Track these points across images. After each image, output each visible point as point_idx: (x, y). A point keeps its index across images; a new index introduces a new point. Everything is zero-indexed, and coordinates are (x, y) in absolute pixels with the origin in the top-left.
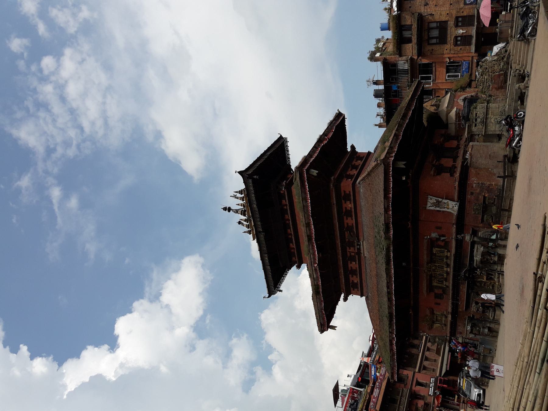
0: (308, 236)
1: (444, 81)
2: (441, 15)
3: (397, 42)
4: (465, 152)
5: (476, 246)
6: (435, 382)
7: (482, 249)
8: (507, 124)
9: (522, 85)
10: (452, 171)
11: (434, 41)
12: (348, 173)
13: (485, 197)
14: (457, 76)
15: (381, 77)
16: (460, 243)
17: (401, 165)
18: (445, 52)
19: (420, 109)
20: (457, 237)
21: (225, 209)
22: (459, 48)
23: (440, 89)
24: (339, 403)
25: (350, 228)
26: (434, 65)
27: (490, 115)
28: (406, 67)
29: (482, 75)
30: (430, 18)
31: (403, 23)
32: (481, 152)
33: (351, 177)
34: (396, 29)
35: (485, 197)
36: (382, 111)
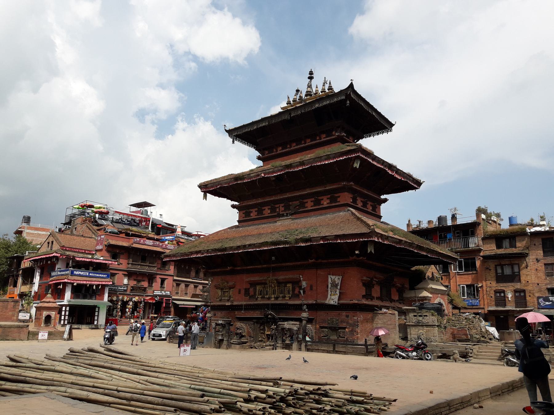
0: (291, 164)
1: (458, 283)
2: (527, 275)
3: (497, 235)
4: (388, 308)
5: (298, 323)
6: (166, 296)
7: (295, 328)
8: (418, 345)
9: (457, 356)
10: (367, 296)
11: (499, 271)
12: (358, 198)
13: (345, 328)
14: (464, 295)
15: (459, 221)
16: (299, 308)
17: (370, 249)
18: (488, 282)
19: (428, 262)
20: (304, 305)
21: (311, 73)
22: (493, 296)
23: (450, 280)
24: (134, 209)
25: (302, 205)
26: (475, 272)
27: (426, 328)
28: (472, 246)
29: (466, 318)
30: (524, 265)
31: (517, 239)
32: (389, 323)
33: (355, 201)
34: (511, 233)
35: (345, 328)
36: (425, 225)
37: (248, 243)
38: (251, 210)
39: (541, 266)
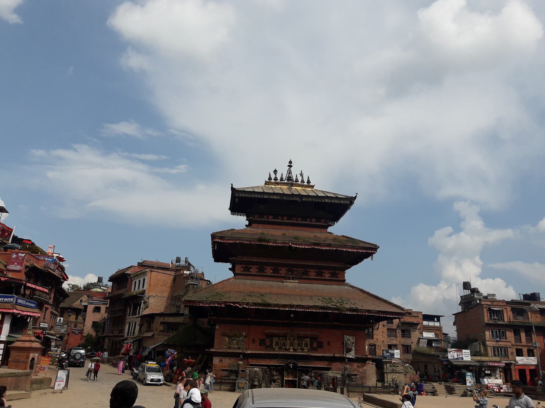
0: (320, 243)
7: (339, 376)
21: (290, 162)
25: (306, 273)
35: (356, 375)
37: (295, 303)
38: (251, 266)
39: (385, 329)
